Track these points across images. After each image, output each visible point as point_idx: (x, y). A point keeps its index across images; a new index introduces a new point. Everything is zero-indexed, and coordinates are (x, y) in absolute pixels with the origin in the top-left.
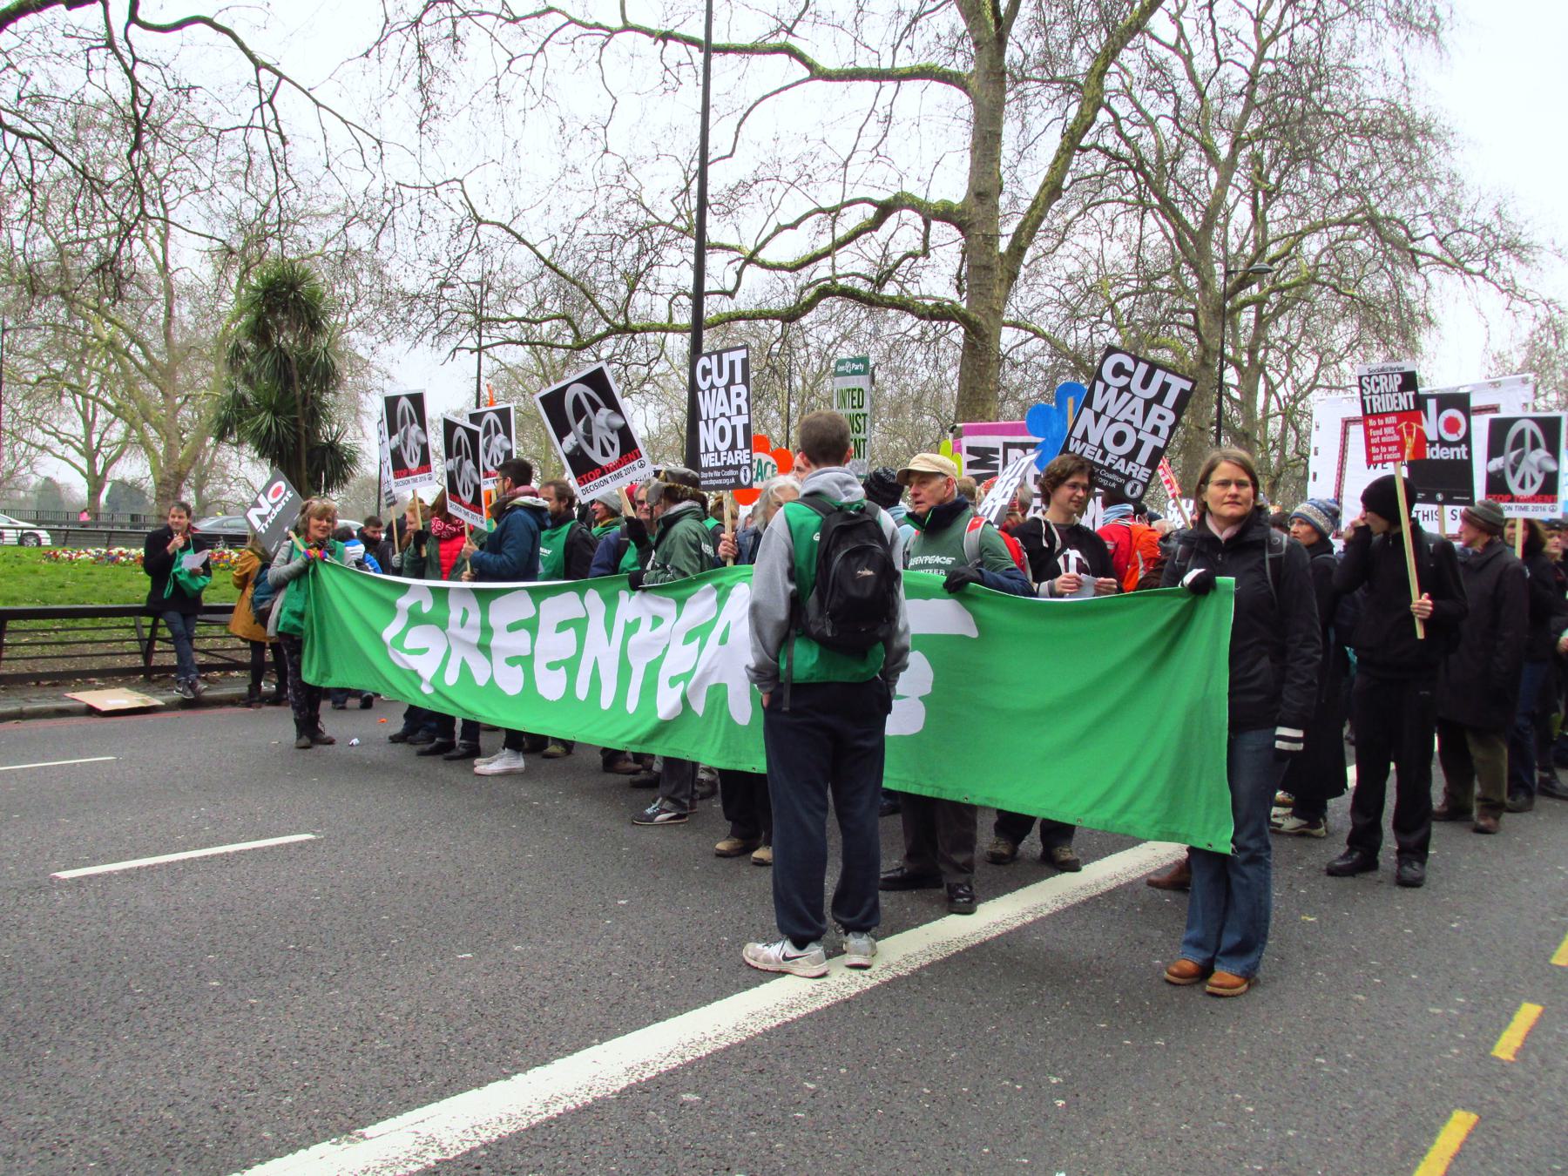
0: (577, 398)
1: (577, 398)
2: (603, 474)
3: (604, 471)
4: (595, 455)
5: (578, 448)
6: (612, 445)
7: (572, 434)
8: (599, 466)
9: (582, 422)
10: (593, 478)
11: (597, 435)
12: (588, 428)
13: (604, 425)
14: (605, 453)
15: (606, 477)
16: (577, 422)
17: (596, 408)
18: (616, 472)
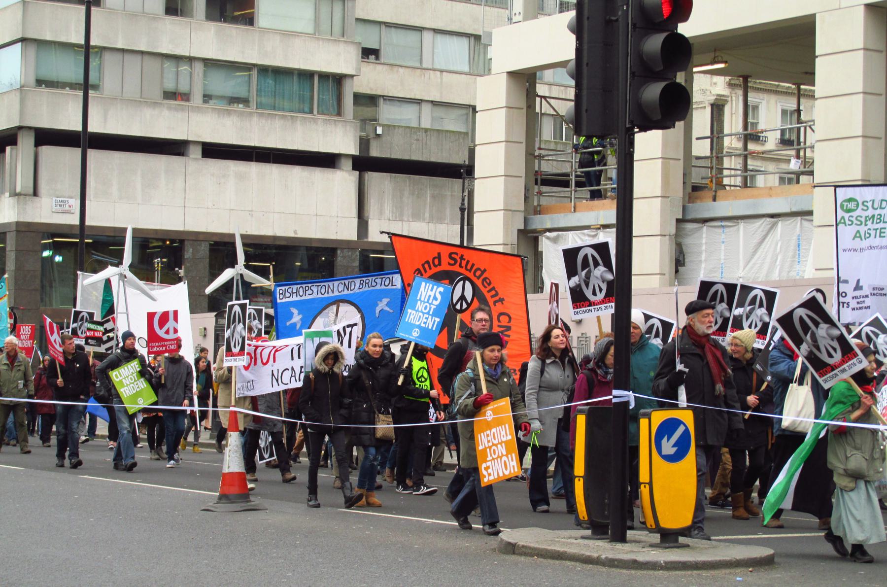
0: (586, 256)
1: (586, 256)
2: (590, 305)
3: (591, 304)
4: (588, 293)
5: (579, 286)
6: (601, 290)
7: (577, 277)
8: (589, 300)
9: (585, 271)
10: (583, 306)
11: (593, 281)
12: (588, 276)
13: (599, 276)
14: (594, 293)
15: (592, 308)
16: (583, 270)
17: (596, 264)
18: (598, 307)
